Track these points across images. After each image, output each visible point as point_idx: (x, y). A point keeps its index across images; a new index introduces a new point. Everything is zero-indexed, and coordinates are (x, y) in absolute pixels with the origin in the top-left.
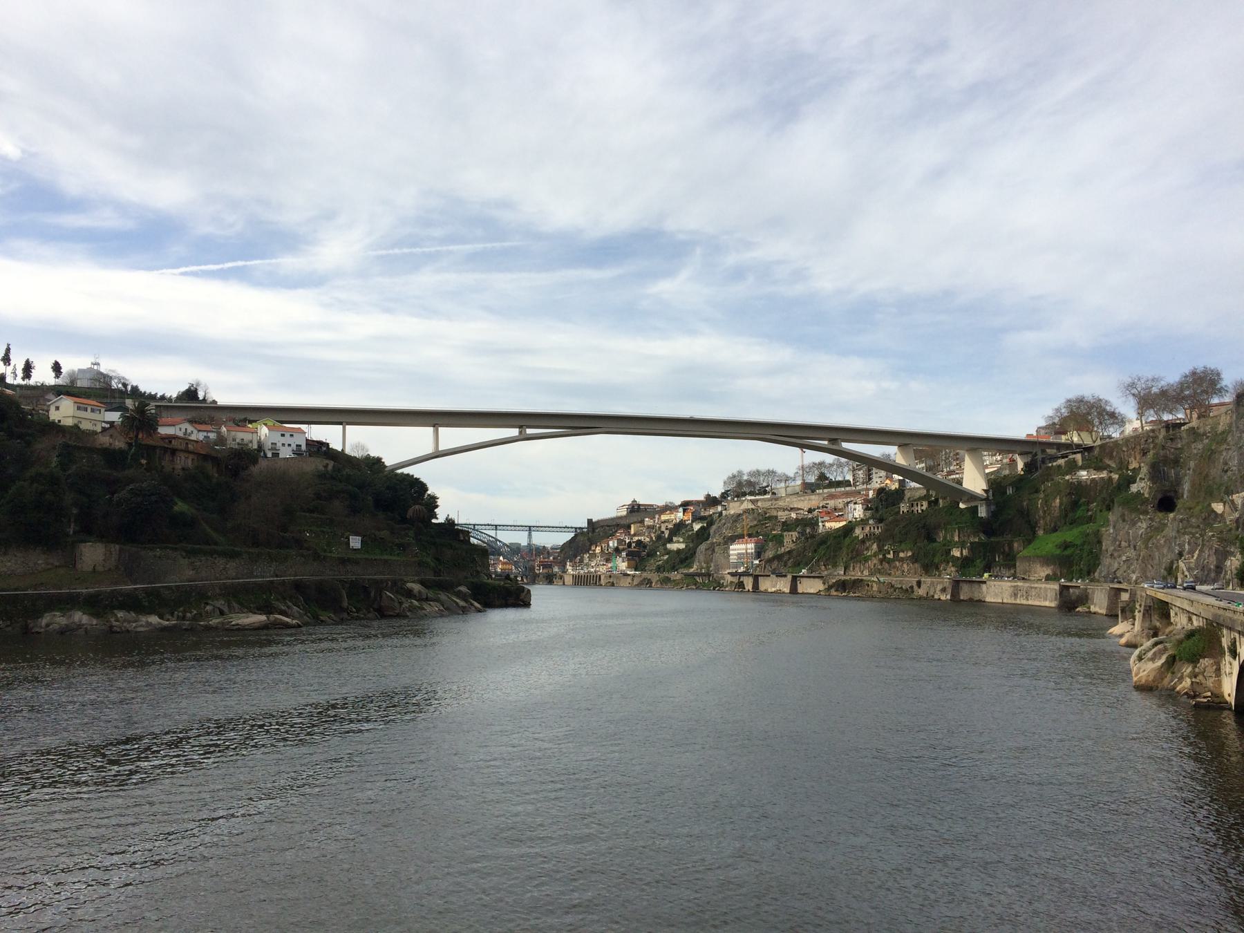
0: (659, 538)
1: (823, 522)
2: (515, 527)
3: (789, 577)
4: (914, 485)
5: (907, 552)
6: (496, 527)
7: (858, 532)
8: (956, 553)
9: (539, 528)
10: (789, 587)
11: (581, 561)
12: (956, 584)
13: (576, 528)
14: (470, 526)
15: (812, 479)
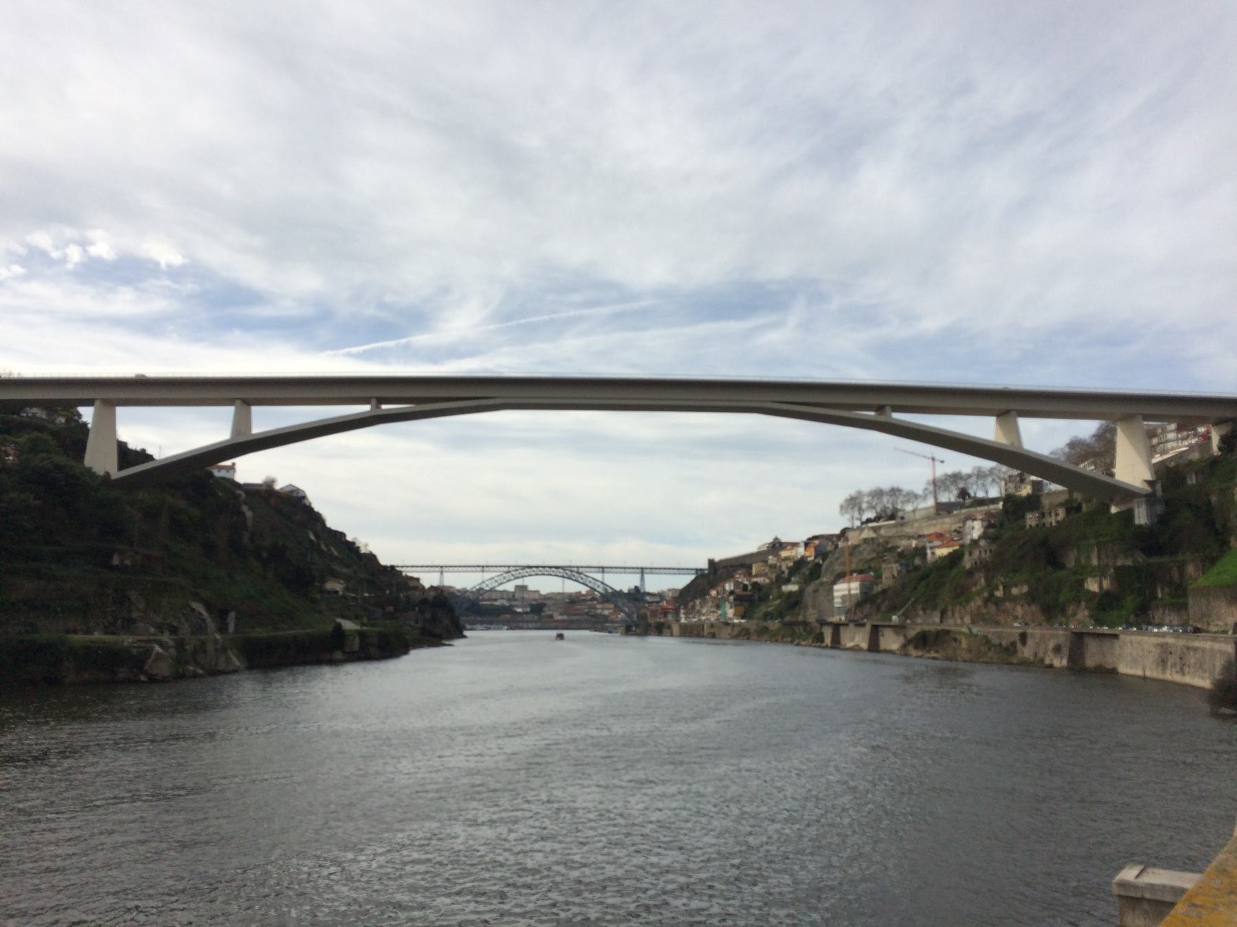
0: (778, 578)
1: (931, 548)
2: (624, 569)
3: (868, 627)
4: (1054, 487)
5: (1022, 586)
6: (603, 569)
7: (967, 563)
8: (1092, 586)
9: (653, 570)
10: (867, 641)
11: (693, 607)
12: (1079, 638)
13: (697, 570)
14: (573, 569)
15: (948, 497)
